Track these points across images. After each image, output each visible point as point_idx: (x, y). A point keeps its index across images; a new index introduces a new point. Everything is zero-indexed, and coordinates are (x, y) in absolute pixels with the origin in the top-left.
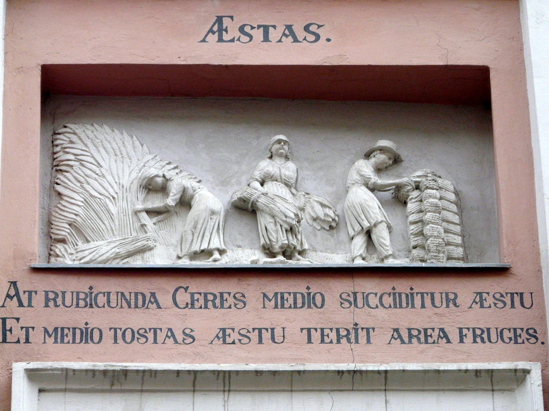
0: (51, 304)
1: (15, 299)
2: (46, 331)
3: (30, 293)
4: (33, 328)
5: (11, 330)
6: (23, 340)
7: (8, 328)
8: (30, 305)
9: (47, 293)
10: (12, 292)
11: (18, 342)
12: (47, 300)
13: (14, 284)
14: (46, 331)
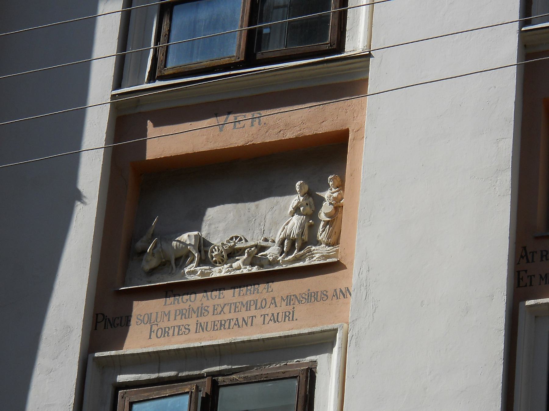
0: (544, 259)
1: (525, 258)
2: (541, 276)
3: (533, 252)
4: (534, 276)
5: (522, 279)
6: (528, 284)
7: (521, 277)
8: (533, 261)
9: (542, 252)
10: (524, 254)
11: (526, 286)
12: (542, 256)
13: (525, 248)
14: (541, 276)
